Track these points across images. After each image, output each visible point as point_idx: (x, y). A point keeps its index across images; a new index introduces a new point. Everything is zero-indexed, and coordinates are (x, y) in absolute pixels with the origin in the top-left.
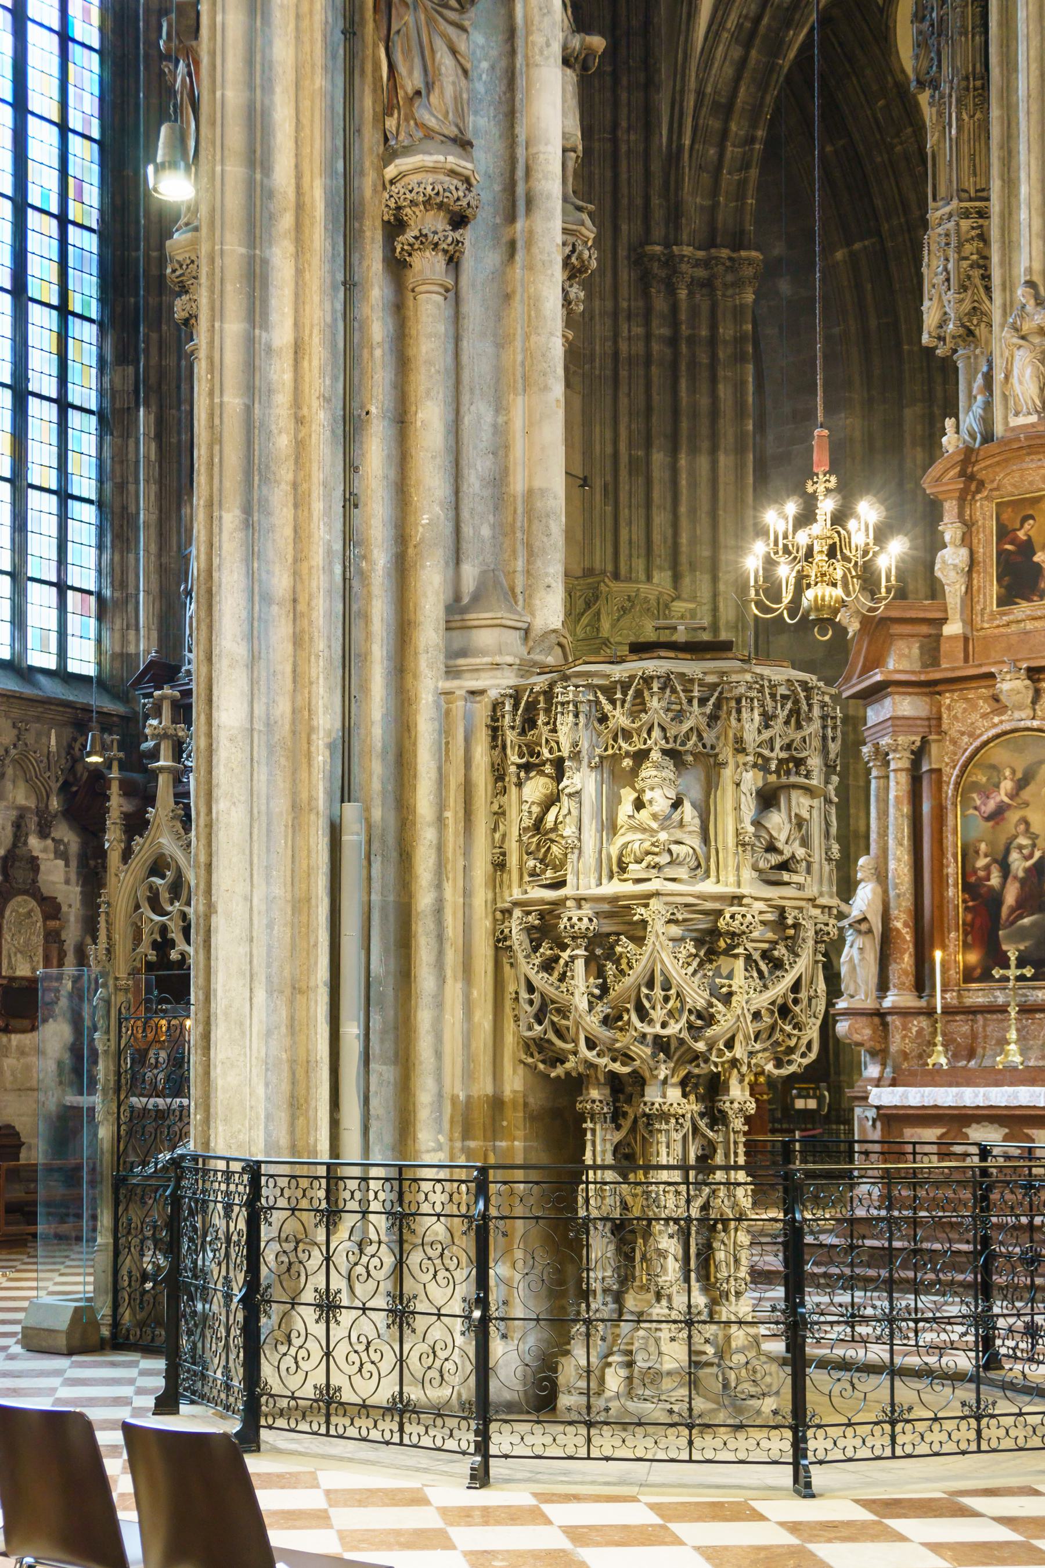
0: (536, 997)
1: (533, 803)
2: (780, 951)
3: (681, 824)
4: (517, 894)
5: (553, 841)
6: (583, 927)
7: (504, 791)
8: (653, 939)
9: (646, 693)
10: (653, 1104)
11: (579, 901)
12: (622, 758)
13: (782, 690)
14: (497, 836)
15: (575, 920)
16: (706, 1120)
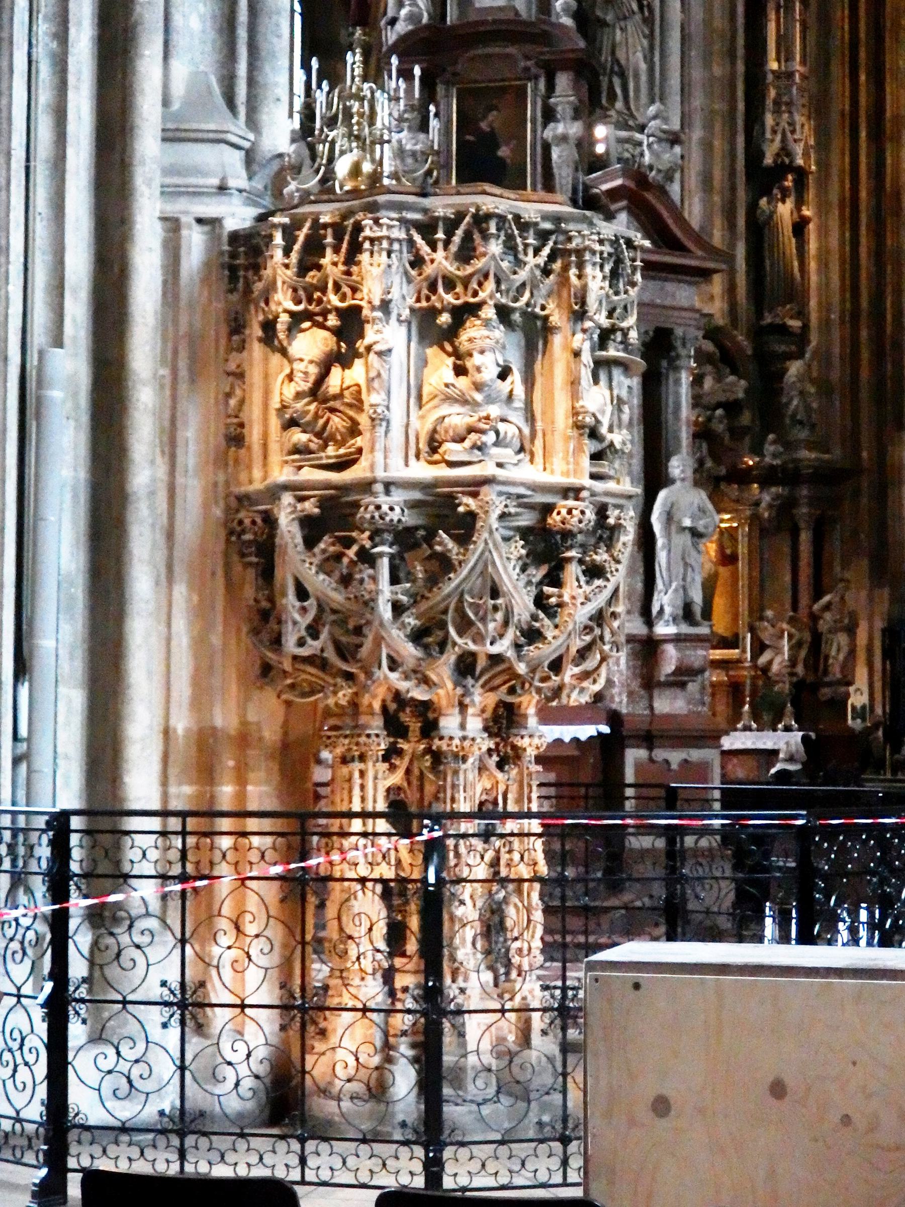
0: (311, 603)
1: (311, 362)
2: (601, 557)
3: (510, 396)
4: (282, 474)
5: (333, 410)
6: (396, 519)
7: (241, 348)
8: (486, 535)
9: (477, 236)
10: (451, 738)
11: (388, 486)
12: (440, 312)
13: (607, 249)
14: (233, 402)
15: (385, 508)
16: (495, 758)
